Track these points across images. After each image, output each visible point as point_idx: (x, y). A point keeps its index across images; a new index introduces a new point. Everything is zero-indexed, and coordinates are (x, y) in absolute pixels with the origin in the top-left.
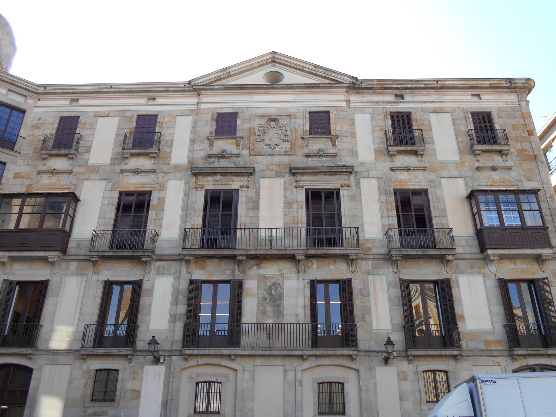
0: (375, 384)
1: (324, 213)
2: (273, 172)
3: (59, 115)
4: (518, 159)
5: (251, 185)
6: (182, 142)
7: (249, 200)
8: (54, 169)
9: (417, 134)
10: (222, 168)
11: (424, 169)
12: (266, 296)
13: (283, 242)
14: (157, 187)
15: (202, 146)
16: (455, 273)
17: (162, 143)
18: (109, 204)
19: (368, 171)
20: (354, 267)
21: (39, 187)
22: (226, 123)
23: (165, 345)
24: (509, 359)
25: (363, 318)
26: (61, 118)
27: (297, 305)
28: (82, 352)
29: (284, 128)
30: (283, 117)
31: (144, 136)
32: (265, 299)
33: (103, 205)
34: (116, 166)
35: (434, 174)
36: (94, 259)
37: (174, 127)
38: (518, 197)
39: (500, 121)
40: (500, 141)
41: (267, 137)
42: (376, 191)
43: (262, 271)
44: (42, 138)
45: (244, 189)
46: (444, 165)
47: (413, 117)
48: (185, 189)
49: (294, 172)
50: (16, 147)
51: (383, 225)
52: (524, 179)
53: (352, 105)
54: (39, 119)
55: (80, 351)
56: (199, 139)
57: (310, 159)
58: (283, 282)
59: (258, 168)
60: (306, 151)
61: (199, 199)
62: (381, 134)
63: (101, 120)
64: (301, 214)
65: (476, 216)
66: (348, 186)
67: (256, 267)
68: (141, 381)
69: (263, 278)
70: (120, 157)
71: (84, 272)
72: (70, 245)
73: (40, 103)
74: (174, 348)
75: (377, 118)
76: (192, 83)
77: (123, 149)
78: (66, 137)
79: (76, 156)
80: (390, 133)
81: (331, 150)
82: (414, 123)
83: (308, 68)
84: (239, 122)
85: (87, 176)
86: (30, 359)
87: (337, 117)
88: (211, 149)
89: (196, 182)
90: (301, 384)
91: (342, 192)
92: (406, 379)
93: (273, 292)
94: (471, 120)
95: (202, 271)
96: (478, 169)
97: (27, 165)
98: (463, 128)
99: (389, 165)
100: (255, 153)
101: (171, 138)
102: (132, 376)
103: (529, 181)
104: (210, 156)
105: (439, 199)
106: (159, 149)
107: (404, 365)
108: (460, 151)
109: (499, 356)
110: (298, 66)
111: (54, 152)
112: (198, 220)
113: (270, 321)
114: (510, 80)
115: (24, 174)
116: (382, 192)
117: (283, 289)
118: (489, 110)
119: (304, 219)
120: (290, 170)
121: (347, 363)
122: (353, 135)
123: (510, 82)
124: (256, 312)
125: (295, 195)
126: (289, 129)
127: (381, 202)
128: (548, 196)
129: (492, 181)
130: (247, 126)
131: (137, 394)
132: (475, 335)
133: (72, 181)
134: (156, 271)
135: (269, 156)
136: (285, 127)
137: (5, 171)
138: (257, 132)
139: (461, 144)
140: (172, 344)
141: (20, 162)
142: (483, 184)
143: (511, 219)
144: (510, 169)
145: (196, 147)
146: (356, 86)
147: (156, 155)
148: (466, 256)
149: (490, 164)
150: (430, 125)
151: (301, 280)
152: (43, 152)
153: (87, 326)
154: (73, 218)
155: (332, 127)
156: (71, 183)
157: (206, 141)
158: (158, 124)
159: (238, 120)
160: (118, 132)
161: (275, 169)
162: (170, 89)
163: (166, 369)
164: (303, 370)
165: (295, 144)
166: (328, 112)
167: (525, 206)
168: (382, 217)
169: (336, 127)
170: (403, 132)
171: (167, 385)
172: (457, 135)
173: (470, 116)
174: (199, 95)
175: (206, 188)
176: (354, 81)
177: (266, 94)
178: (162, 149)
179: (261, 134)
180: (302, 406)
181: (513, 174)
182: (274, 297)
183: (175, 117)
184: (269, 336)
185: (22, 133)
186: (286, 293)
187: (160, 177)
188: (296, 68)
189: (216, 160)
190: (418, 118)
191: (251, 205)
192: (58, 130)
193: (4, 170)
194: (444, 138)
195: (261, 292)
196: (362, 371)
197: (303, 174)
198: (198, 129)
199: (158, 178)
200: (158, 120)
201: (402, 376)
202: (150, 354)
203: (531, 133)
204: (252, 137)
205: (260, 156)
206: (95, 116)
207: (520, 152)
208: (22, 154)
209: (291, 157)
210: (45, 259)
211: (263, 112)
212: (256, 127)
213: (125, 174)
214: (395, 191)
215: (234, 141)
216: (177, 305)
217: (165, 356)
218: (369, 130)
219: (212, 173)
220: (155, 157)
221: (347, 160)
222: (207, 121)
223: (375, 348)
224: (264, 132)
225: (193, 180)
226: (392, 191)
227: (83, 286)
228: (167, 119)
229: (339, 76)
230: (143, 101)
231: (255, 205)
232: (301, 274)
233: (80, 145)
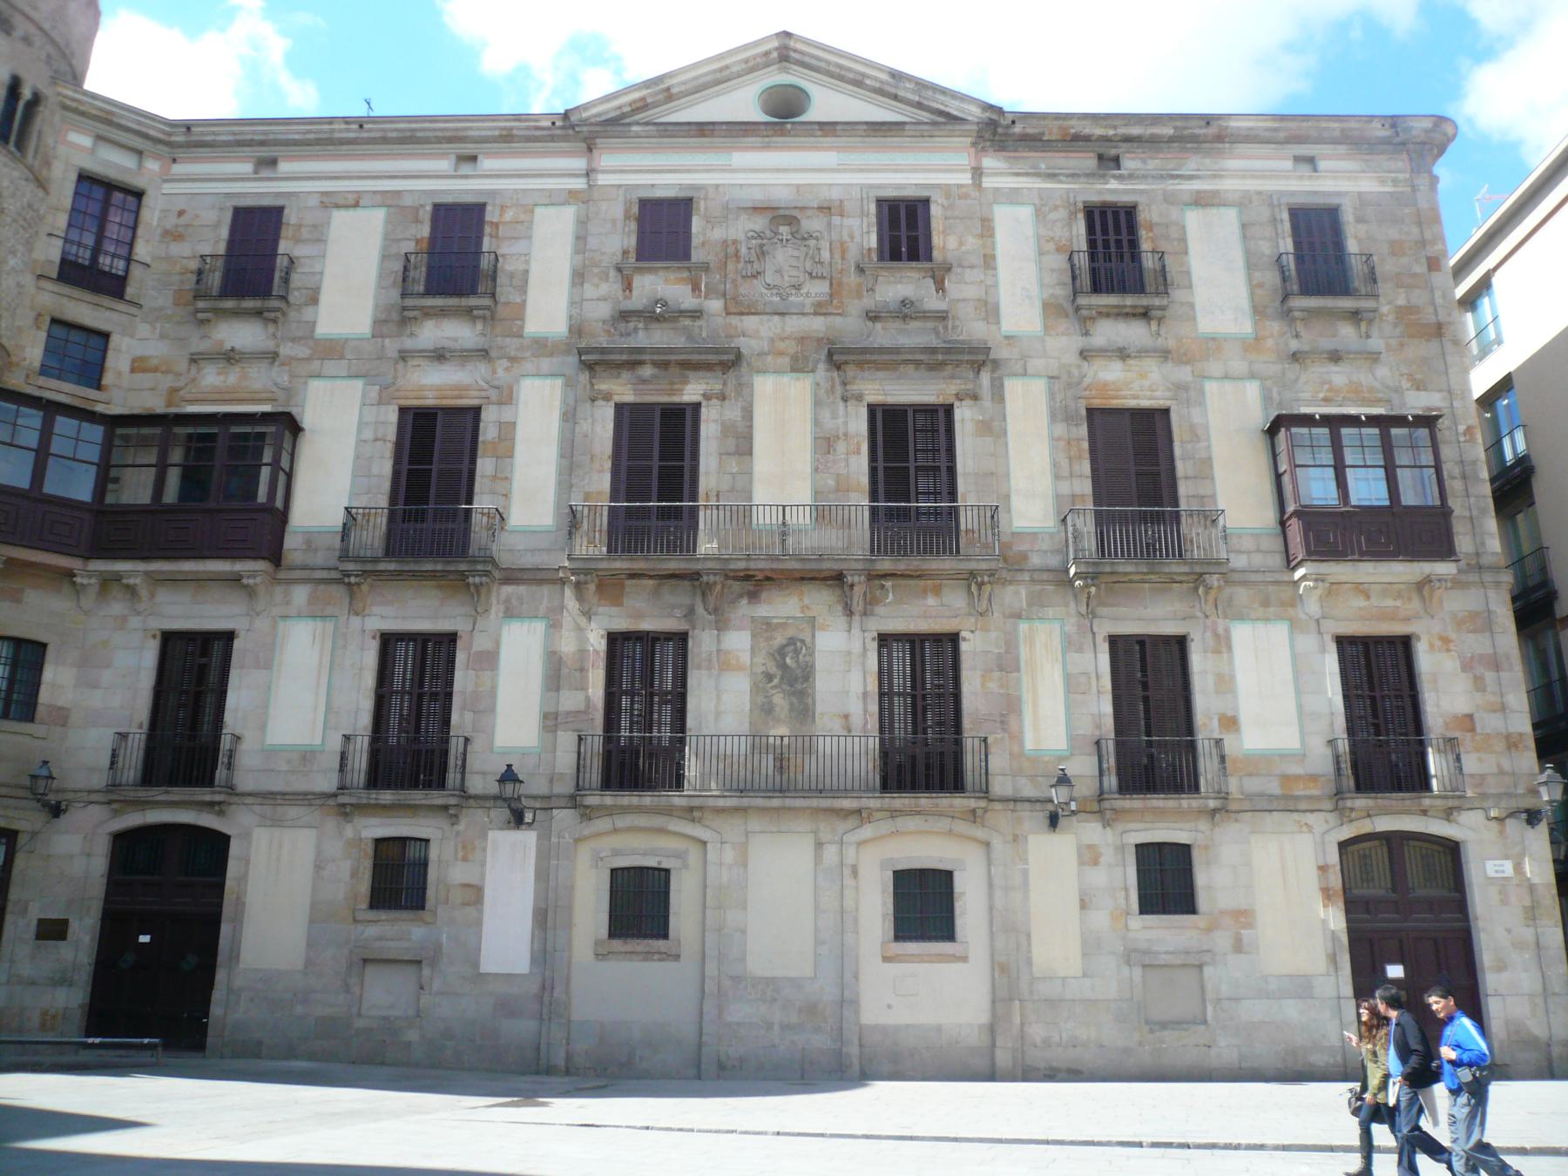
0: (1025, 873)
2: (787, 359)
3: (231, 203)
4: (1398, 331)
5: (730, 390)
6: (551, 275)
7: (727, 429)
8: (233, 350)
9: (1149, 262)
10: (658, 351)
11: (1165, 355)
12: (773, 669)
13: (812, 540)
14: (493, 394)
15: (604, 289)
16: (1226, 617)
17: (502, 280)
18: (376, 440)
19: (1024, 358)
20: (985, 603)
21: (199, 396)
22: (663, 228)
23: (535, 785)
24: (1332, 818)
25: (1002, 722)
26: (238, 212)
27: (847, 693)
28: (342, 799)
29: (812, 243)
30: (809, 213)
31: (453, 261)
32: (769, 677)
33: (361, 442)
34: (387, 341)
35: (1188, 368)
36: (353, 580)
37: (530, 238)
38: (1389, 435)
39: (1362, 229)
40: (1356, 284)
41: (769, 267)
42: (1042, 408)
43: (763, 610)
44: (194, 265)
45: (714, 401)
46: (1214, 345)
47: (1143, 216)
48: (564, 402)
50: (130, 291)
51: (1058, 497)
52: (1405, 384)
53: (988, 182)
54: (181, 213)
55: (335, 795)
56: (596, 270)
57: (879, 326)
58: (813, 636)
59: (747, 345)
60: (868, 302)
61: (601, 428)
62: (1059, 262)
63: (339, 217)
64: (860, 466)
66: (975, 397)
67: (744, 601)
68: (483, 864)
69: (764, 627)
70: (395, 316)
71: (329, 610)
72: (290, 542)
73: (177, 169)
74: (557, 789)
75: (1052, 216)
76: (574, 118)
77: (403, 295)
78: (253, 264)
79: (284, 314)
80: (1083, 260)
81: (933, 303)
82: (1143, 233)
83: (876, 79)
84: (697, 224)
85: (316, 364)
86: (221, 813)
87: (949, 214)
88: (626, 298)
89: (592, 385)
90: (855, 872)
91: (958, 414)
92: (1095, 863)
93: (788, 660)
94: (1287, 226)
95: (614, 610)
96: (1295, 357)
97: (162, 336)
98: (1265, 248)
99: (1078, 342)
100: (739, 307)
101: (522, 267)
102: (460, 854)
103: (1418, 389)
104: (624, 316)
105: (1195, 435)
106: (493, 295)
107: (1092, 831)
108: (1258, 311)
109: (1312, 811)
110: (850, 75)
111: (229, 304)
112: (602, 482)
113: (783, 730)
114: (1394, 121)
115: (155, 362)
116: (1058, 414)
117: (812, 654)
118: (1334, 201)
119: (865, 480)
120: (830, 354)
121: (962, 827)
122: (989, 261)
123: (1394, 126)
124: (747, 707)
125: (840, 421)
126: (825, 245)
127: (1054, 439)
128: (1462, 428)
129: (1330, 390)
130: (717, 234)
131: (475, 894)
132: (1259, 763)
133: (279, 380)
134: (502, 608)
135: (776, 318)
136: (817, 239)
137: (110, 355)
138: (744, 250)
139: (1259, 292)
140: (551, 781)
141: (143, 329)
142: (1307, 395)
143: (1368, 489)
144: (1374, 358)
145: (589, 291)
146: (1000, 131)
147: (487, 313)
148: (1253, 577)
149: (1327, 344)
150: (1183, 240)
151: (856, 631)
152: (201, 304)
153: (347, 738)
154: (290, 476)
155: (936, 240)
156: (276, 384)
157: (612, 273)
158: (487, 230)
159: (695, 220)
160: (385, 248)
161: (792, 351)
162: (517, 134)
163: (539, 838)
164: (859, 844)
165: (840, 284)
166: (926, 202)
167: (1402, 457)
168: (1057, 477)
169: (945, 239)
170: (1115, 258)
171: (542, 875)
172: (1251, 265)
173: (1286, 216)
174: (590, 150)
175: (617, 399)
176: (994, 117)
177: (767, 147)
178: (502, 298)
179: (753, 258)
180: (856, 921)
181: (1382, 372)
182: (791, 674)
183: (530, 211)
184: (781, 763)
185: (142, 251)
186: (820, 663)
187: (500, 372)
188: (841, 78)
189: (641, 325)
190: (1156, 219)
191: (731, 443)
192: (231, 243)
193: (105, 351)
194: (1217, 271)
195: (759, 659)
196: (997, 843)
197: (861, 365)
198: (593, 242)
199: (494, 372)
200: (488, 218)
201: (1089, 856)
202: (499, 803)
203: (1434, 264)
204: (731, 266)
205: (753, 318)
206: (324, 206)
207: (1404, 312)
208: (145, 309)
209: (831, 319)
210: (235, 580)
211: (758, 196)
212: (741, 237)
213: (411, 362)
214: (1091, 412)
215: (685, 274)
216: (558, 689)
217: (535, 810)
218: (1030, 250)
219: (631, 362)
220: (484, 318)
221: (973, 329)
222: (614, 222)
223: (1028, 791)
224: (762, 253)
225: (584, 377)
226: (1084, 413)
227: (328, 644)
228: (509, 215)
229: (956, 103)
230: (444, 165)
232: (856, 618)
233: (292, 285)
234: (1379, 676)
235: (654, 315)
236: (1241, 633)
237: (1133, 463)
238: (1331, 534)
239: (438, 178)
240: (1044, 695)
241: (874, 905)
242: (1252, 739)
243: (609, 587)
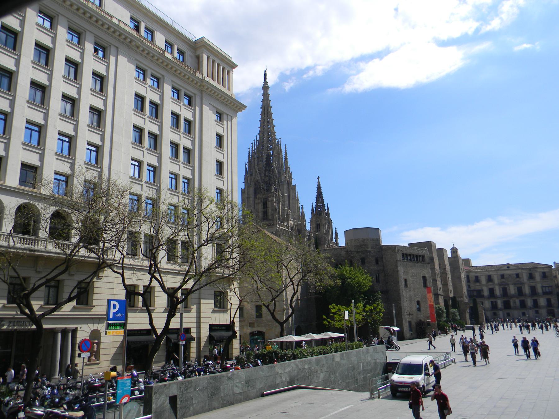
6: (496, 280)
22: (502, 276)
31: (490, 279)
61: (501, 289)
64: (517, 290)
65: (542, 290)
112: (502, 292)
143: (547, 290)
169: (520, 276)
182: (515, 302)
185: (470, 279)
194: (538, 277)
231: (509, 289)
234: (549, 301)
235: (503, 282)
237: (533, 290)
238: (545, 293)
241: (521, 314)
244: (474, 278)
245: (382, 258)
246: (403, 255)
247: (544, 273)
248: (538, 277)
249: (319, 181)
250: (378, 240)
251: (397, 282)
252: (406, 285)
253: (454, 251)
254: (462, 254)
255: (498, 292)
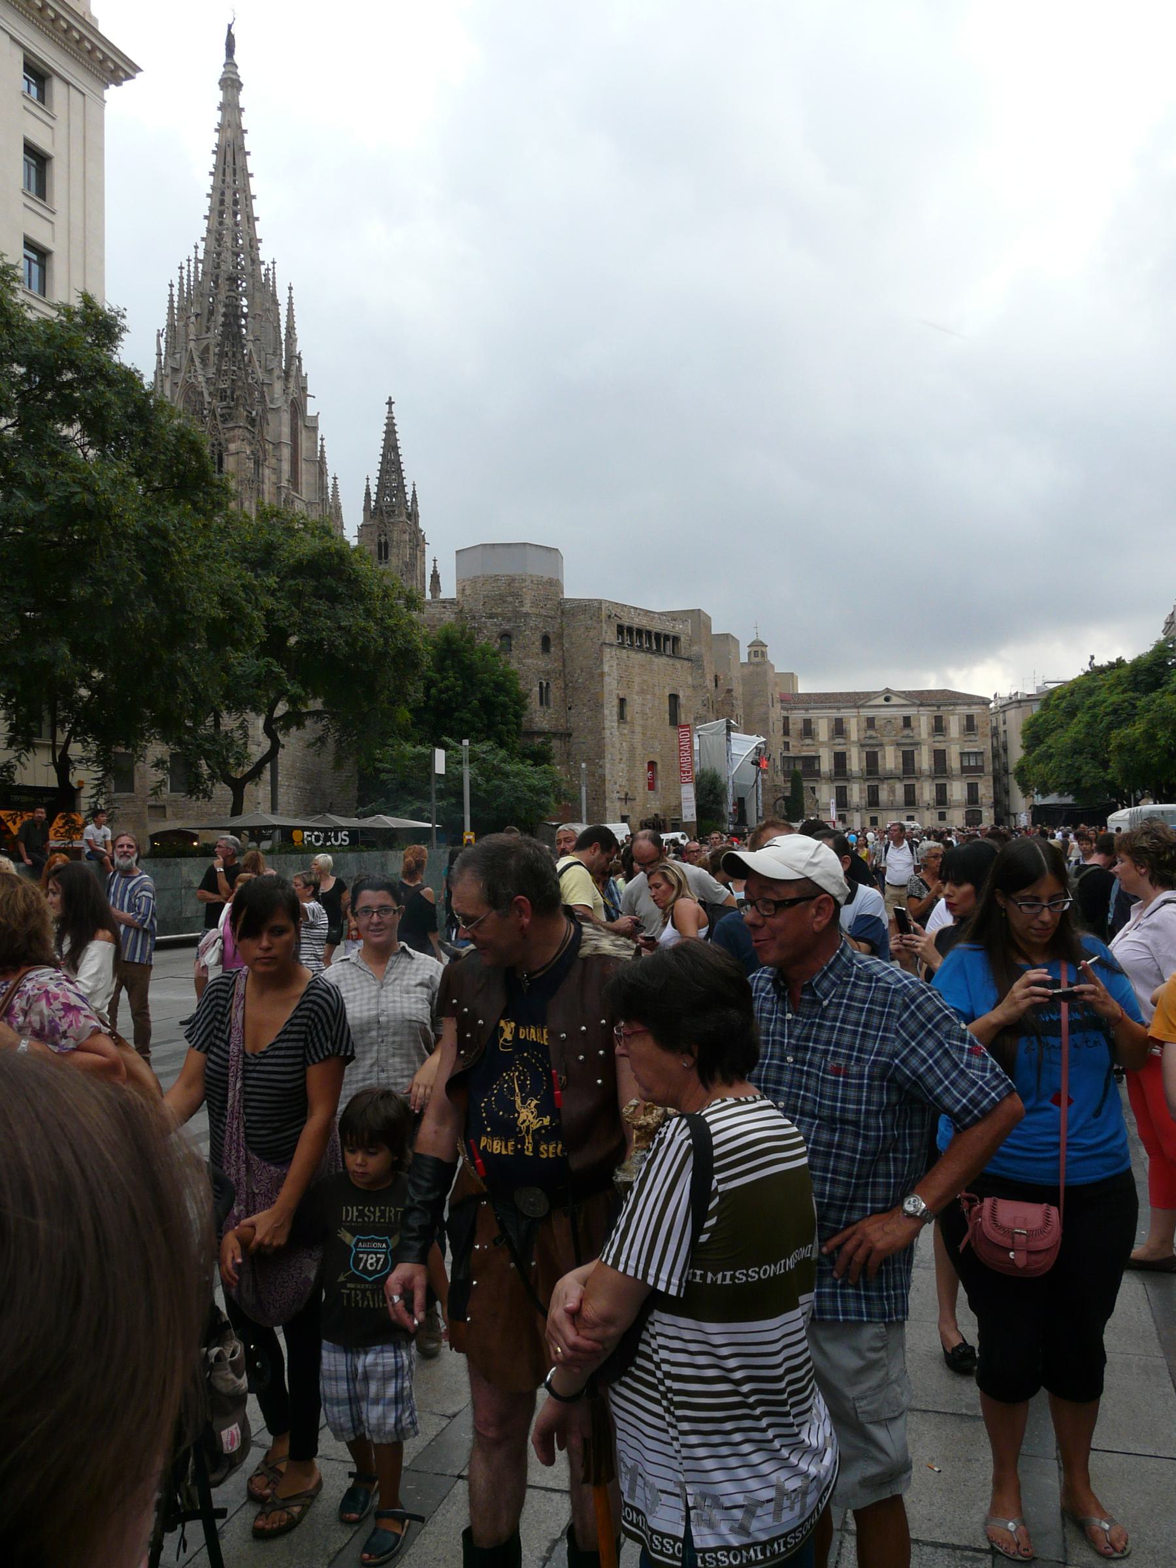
1: (908, 759)
6: (854, 730)
22: (871, 722)
31: (839, 729)
46: (953, 739)
49: (898, 745)
143: (973, 763)
169: (913, 724)
182: (892, 791)
185: (791, 727)
194: (954, 726)
221: (917, 738)
234: (972, 789)
235: (871, 738)
236: (954, 783)
239: (835, 714)
240: (926, 792)
242: (955, 798)
243: (868, 779)
244: (800, 726)
245: (560, 636)
246: (620, 629)
247: (970, 718)
248: (954, 726)
249: (390, 412)
250: (555, 584)
251: (597, 706)
252: (622, 716)
253: (758, 649)
254: (779, 663)
255: (855, 763)
